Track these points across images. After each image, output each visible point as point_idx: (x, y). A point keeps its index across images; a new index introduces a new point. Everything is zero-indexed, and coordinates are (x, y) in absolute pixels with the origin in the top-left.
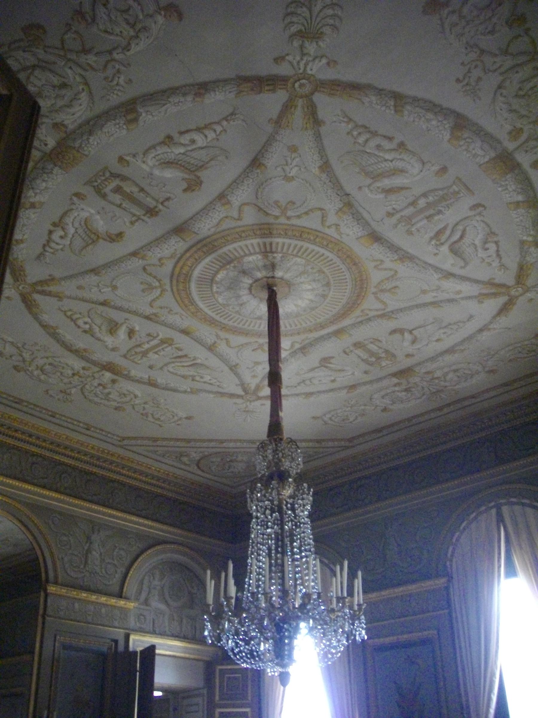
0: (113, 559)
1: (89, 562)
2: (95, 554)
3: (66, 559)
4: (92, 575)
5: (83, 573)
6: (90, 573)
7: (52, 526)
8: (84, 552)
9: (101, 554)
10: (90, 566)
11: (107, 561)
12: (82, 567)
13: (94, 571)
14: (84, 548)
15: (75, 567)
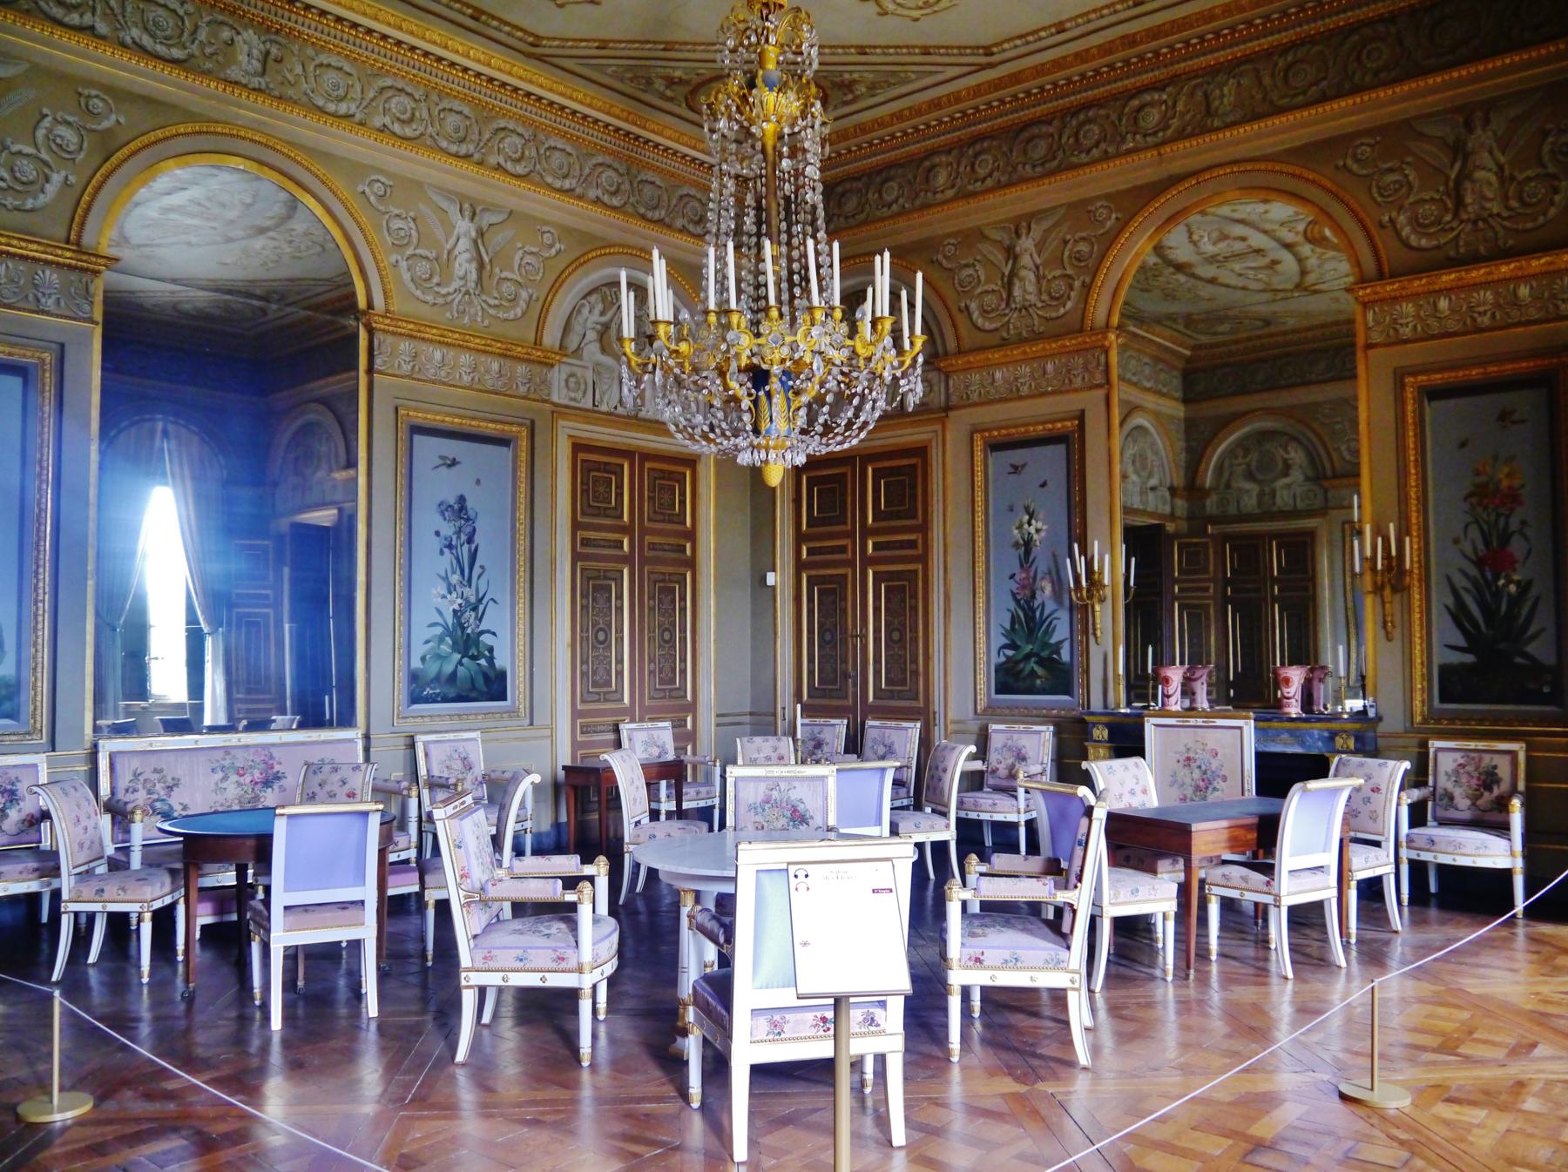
0: (1544, 166)
1: (1469, 200)
2: (1486, 176)
3: (1402, 219)
4: (1481, 224)
5: (1452, 229)
6: (1475, 222)
7: (1355, 167)
8: (1451, 184)
9: (1501, 167)
10: (1470, 209)
11: (1521, 177)
12: (1448, 218)
13: (1485, 214)
14: (1448, 178)
15: (1426, 226)
